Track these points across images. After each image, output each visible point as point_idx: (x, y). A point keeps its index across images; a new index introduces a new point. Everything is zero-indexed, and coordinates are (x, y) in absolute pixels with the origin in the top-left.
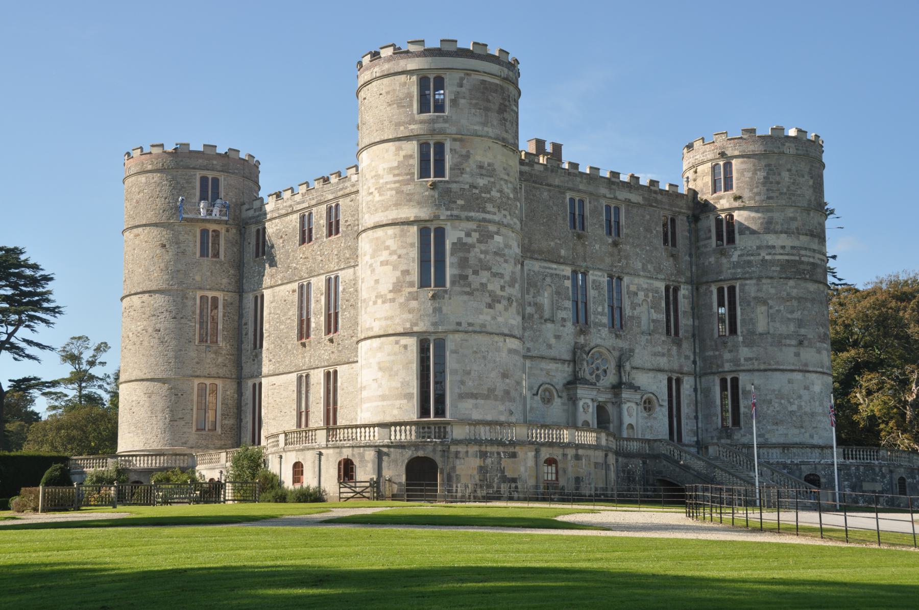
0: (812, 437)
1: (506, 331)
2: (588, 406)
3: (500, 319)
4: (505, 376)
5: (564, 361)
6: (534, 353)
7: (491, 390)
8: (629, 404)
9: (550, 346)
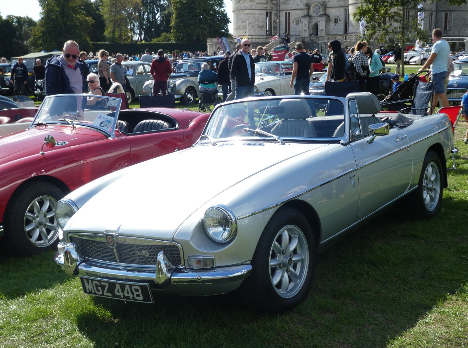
0: (357, 29)
1: (244, 8)
2: (306, 24)
3: (241, 5)
4: (243, 22)
5: (302, 9)
6: (293, 8)
7: (239, 27)
8: (320, 22)
9: (298, 5)
